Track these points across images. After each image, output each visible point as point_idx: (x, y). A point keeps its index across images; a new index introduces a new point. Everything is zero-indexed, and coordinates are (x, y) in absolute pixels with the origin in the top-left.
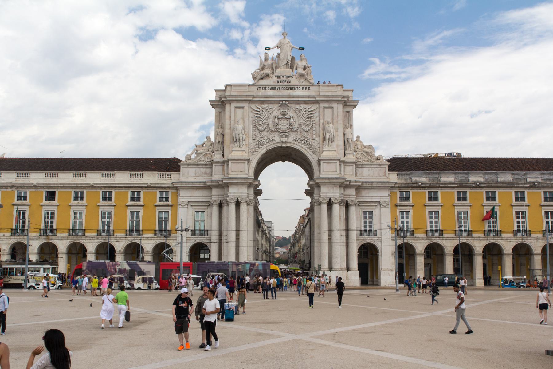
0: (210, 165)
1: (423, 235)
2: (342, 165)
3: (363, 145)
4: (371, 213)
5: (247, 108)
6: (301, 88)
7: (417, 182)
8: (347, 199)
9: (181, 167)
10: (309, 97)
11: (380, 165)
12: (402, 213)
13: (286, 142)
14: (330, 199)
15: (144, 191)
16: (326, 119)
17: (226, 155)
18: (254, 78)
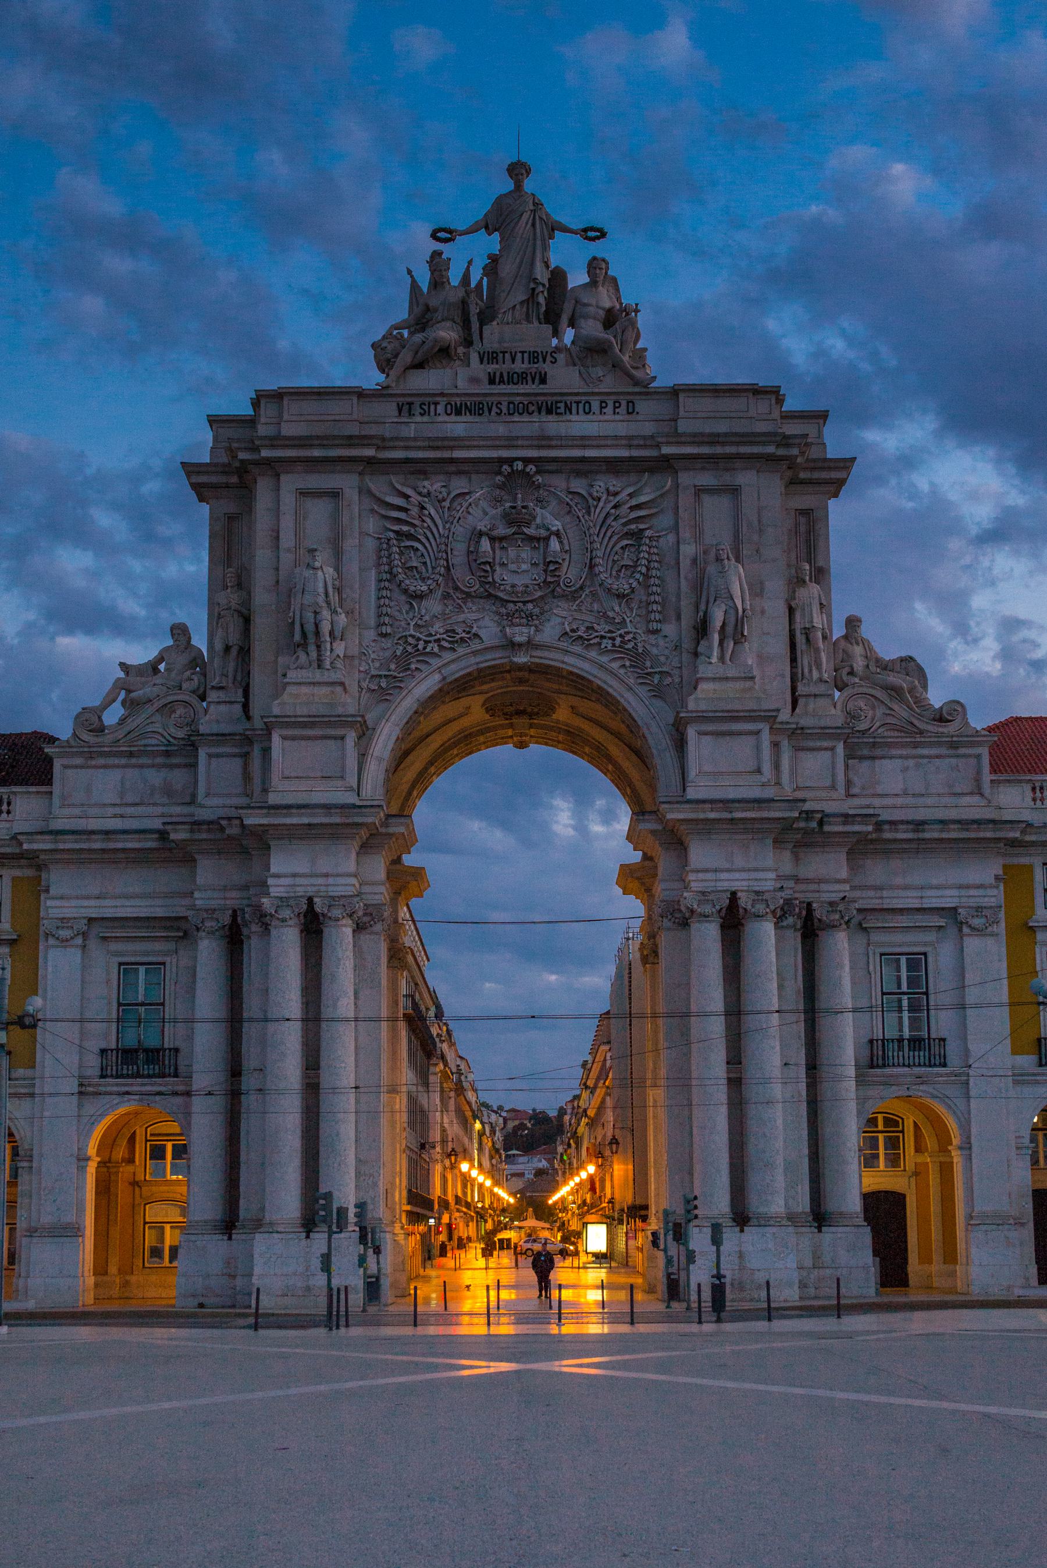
0: (186, 750)
2: (785, 744)
4: (917, 962)
5: (351, 494)
6: (595, 406)
8: (810, 897)
9: (57, 764)
10: (630, 441)
11: (953, 745)
13: (530, 645)
14: (734, 896)
17: (256, 711)
18: (384, 364)
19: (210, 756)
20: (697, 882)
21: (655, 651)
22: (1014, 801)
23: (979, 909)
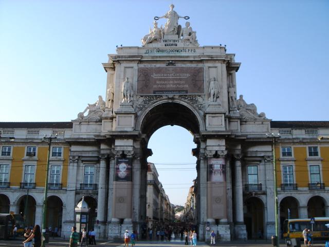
1: (307, 189)
3: (247, 104)
6: (187, 50)
7: (298, 138)
10: (194, 57)
12: (285, 167)
13: (173, 99)
15: (39, 146)
16: (211, 77)
19: (104, 122)
20: (208, 148)
21: (199, 100)
22: (276, 133)
23: (269, 157)
